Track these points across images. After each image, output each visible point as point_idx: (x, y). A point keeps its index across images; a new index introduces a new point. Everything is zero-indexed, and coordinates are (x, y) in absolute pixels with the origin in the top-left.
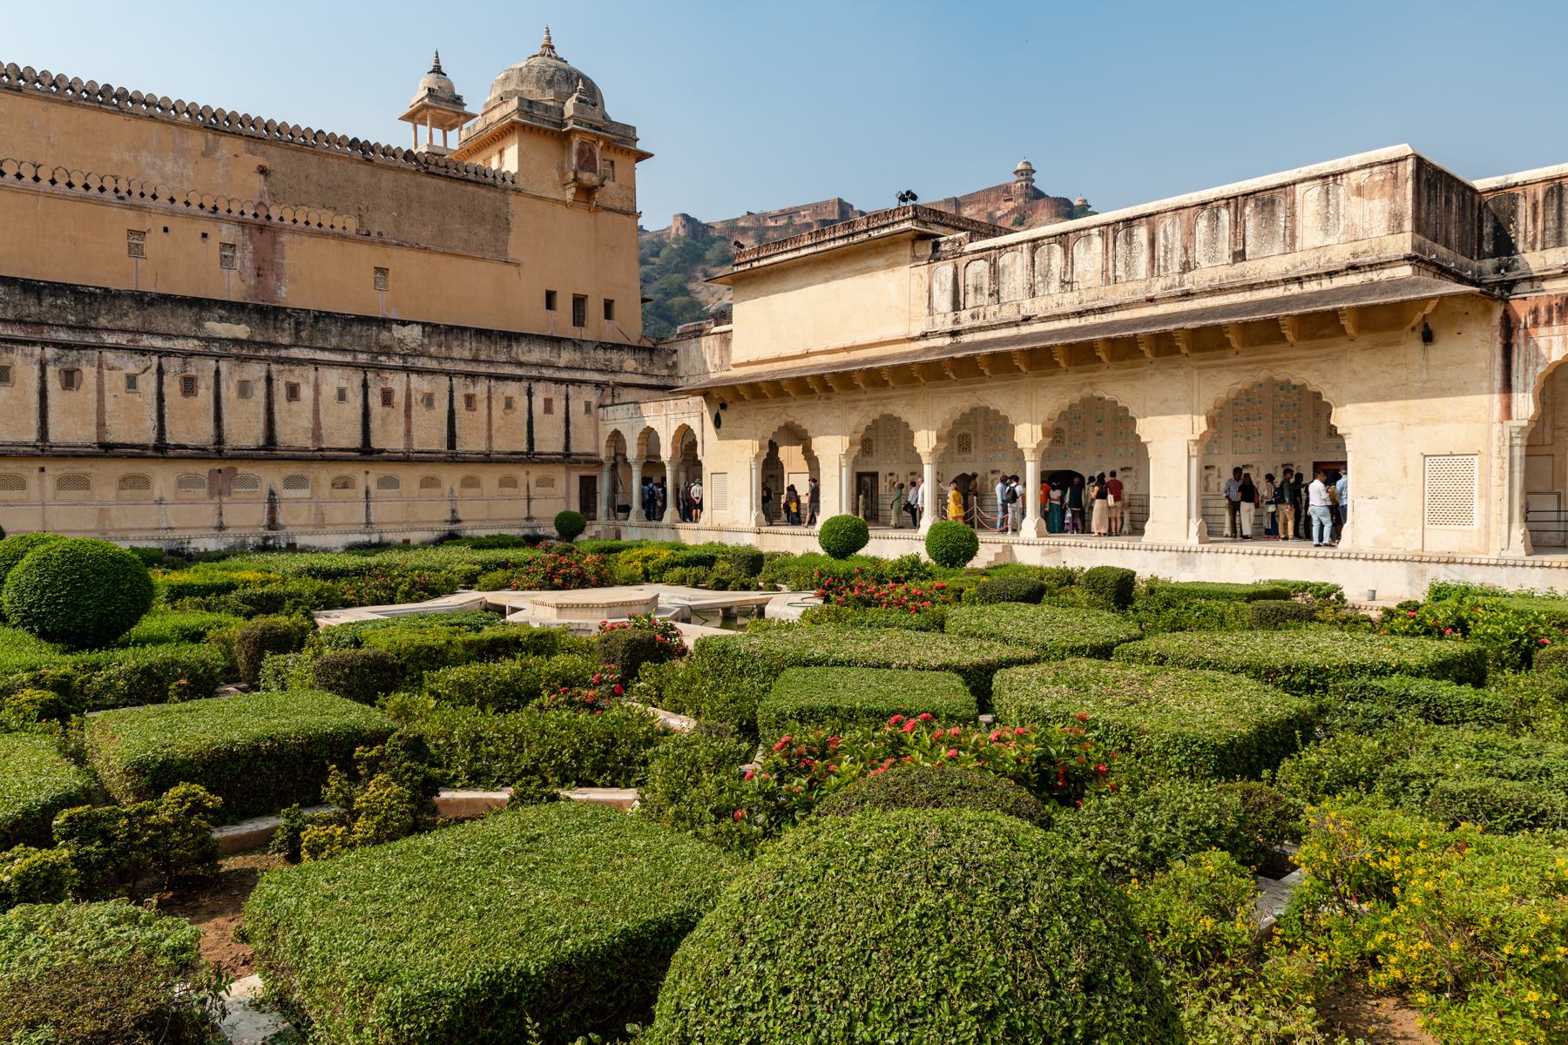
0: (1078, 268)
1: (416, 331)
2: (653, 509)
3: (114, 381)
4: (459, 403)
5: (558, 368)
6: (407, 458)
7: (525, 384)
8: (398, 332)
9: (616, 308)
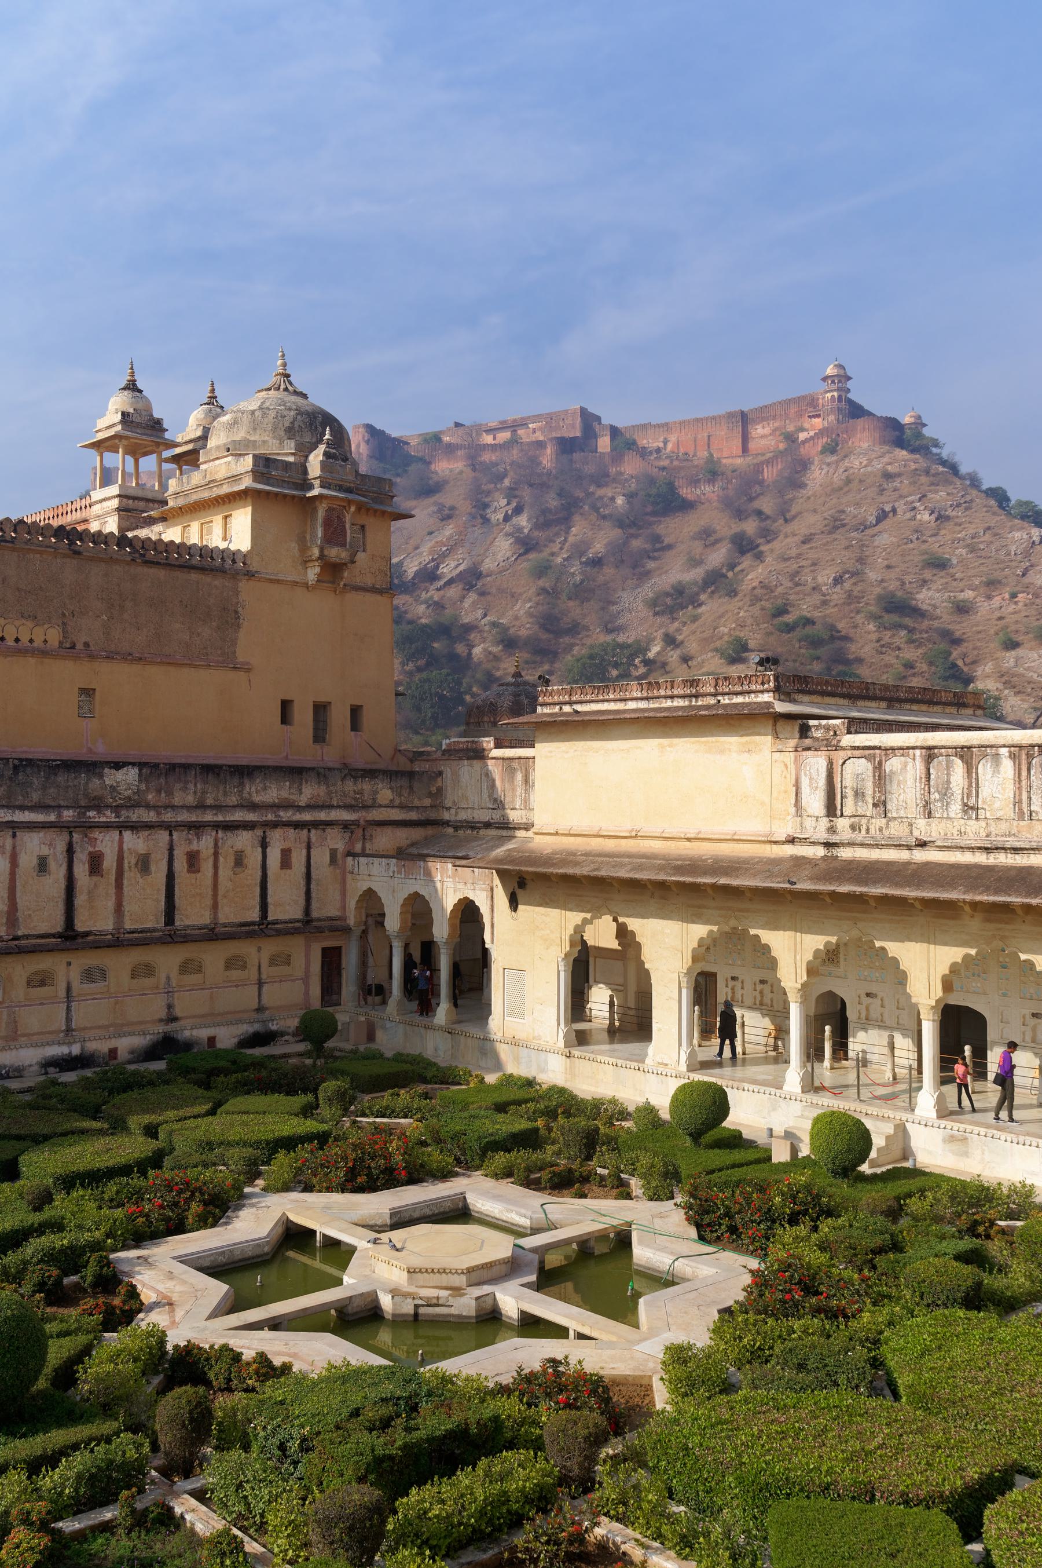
0: (984, 792)
1: (131, 774)
2: (421, 996)
4: (180, 865)
5: (299, 808)
6: (118, 941)
7: (259, 832)
9: (367, 718)
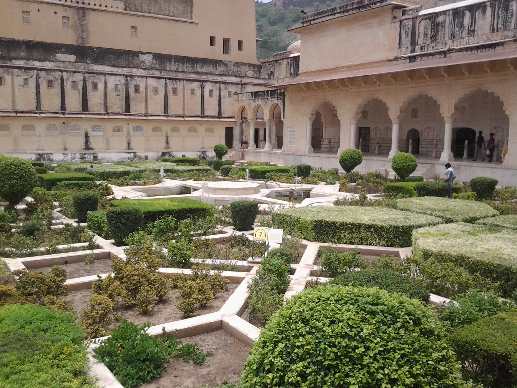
3: (19, 80)
8: (142, 57)
9: (245, 45)
